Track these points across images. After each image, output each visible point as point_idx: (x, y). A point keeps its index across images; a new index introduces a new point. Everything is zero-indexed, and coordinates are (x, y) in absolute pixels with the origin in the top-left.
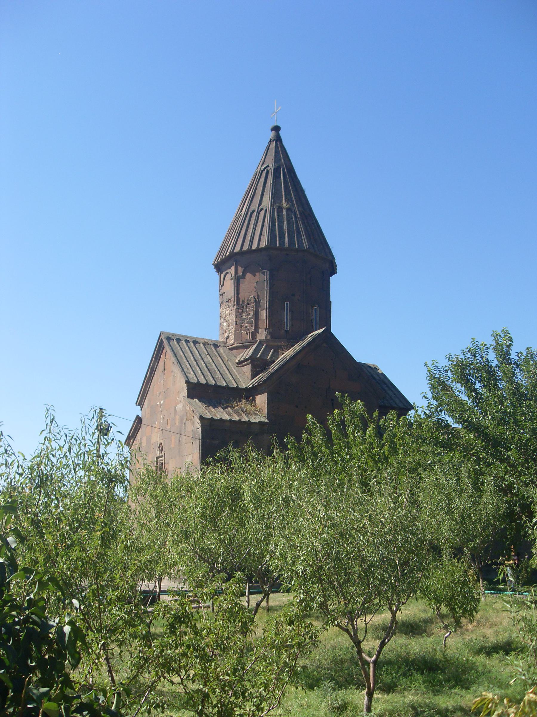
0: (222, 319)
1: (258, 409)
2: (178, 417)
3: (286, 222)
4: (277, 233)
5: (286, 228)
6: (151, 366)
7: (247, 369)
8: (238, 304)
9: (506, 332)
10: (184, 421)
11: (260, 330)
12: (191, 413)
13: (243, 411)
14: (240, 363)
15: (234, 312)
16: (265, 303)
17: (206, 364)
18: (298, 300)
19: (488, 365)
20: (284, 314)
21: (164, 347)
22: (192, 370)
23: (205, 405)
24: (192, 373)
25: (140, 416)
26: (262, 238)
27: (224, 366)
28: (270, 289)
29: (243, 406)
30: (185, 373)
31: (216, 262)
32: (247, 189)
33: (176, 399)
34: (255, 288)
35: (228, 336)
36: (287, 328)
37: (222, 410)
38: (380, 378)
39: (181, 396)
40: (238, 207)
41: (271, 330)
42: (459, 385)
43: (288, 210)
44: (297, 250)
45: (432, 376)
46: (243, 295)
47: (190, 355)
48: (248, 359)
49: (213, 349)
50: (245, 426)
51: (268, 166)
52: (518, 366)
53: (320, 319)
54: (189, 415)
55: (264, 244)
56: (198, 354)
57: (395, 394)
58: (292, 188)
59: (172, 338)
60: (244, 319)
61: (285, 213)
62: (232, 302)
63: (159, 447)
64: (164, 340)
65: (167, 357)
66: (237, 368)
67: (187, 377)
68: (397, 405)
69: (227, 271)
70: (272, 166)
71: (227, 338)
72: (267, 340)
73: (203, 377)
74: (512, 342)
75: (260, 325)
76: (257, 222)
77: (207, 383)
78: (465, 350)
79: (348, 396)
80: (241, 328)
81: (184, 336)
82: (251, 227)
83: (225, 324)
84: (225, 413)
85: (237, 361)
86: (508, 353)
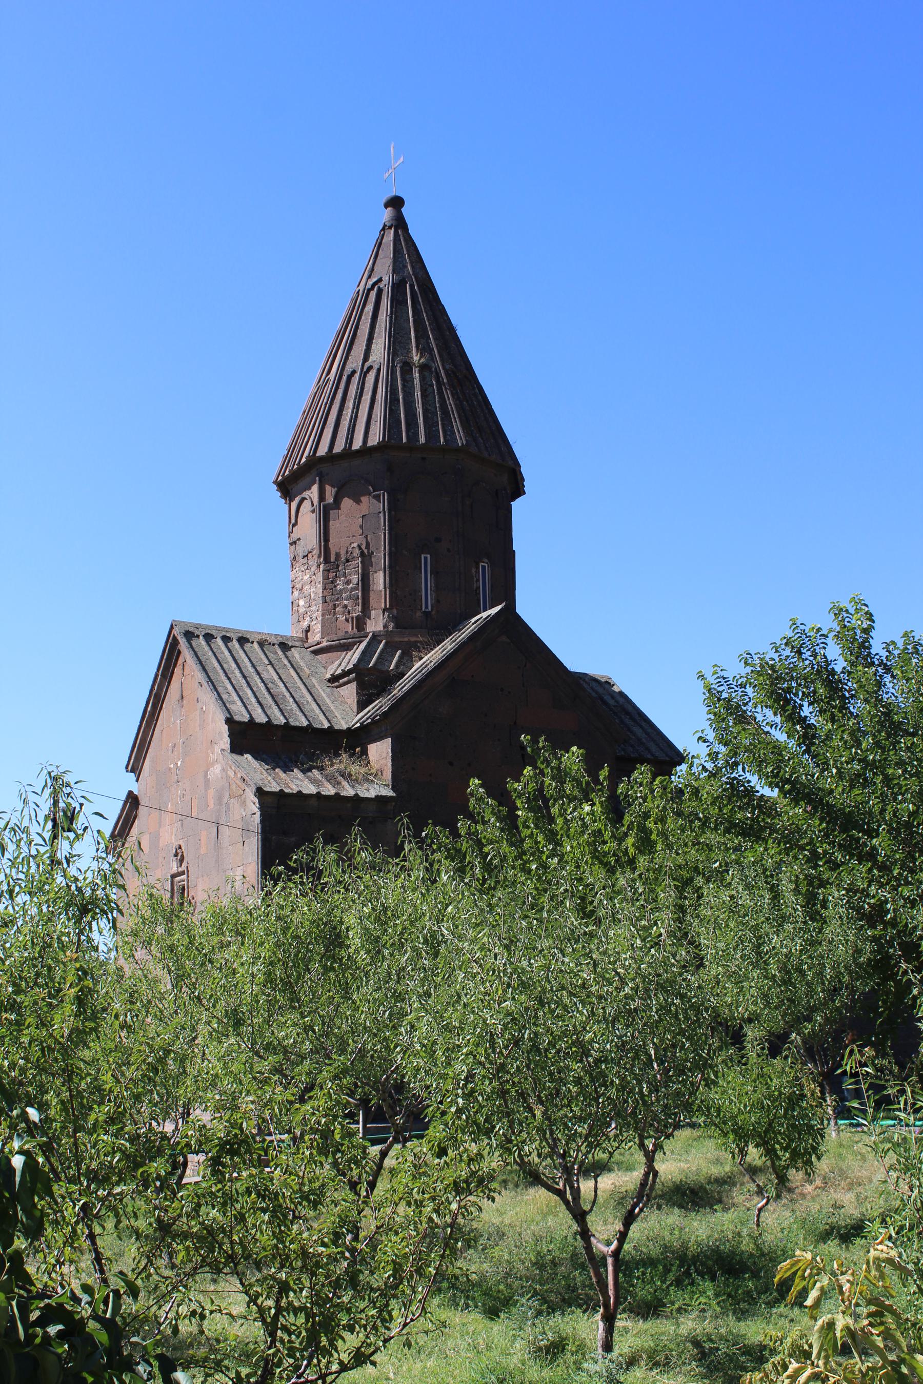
0: (296, 593)
1: (373, 771)
2: (212, 792)
3: (419, 393)
4: (402, 416)
5: (420, 405)
6: (154, 692)
7: (350, 692)
8: (327, 560)
9: (859, 603)
10: (225, 800)
11: (373, 613)
12: (239, 782)
13: (343, 776)
14: (334, 679)
15: (320, 577)
16: (381, 557)
17: (265, 685)
18: (449, 550)
19: (826, 669)
20: (421, 578)
21: (179, 652)
22: (239, 696)
23: (267, 767)
24: (239, 703)
25: (136, 793)
26: (372, 427)
27: (302, 687)
29: (342, 766)
31: (280, 478)
33: (208, 756)
34: (361, 527)
35: (309, 627)
36: (427, 607)
38: (617, 702)
40: (322, 365)
41: (395, 611)
42: (769, 713)
43: (423, 368)
44: (443, 450)
45: (713, 697)
47: (234, 666)
48: (350, 672)
49: (280, 652)
50: (349, 805)
51: (380, 280)
52: (888, 669)
54: (234, 787)
56: (249, 665)
57: (647, 734)
58: (430, 324)
59: (197, 632)
60: (341, 590)
61: (417, 375)
62: (315, 557)
63: (176, 855)
64: (179, 638)
66: (328, 690)
67: (228, 710)
68: (652, 755)
71: (307, 631)
72: (387, 631)
73: (260, 710)
74: (873, 622)
75: (372, 602)
77: (269, 722)
80: (335, 609)
82: (350, 404)
83: (302, 603)
84: (306, 781)
85: (328, 676)
86: (865, 645)
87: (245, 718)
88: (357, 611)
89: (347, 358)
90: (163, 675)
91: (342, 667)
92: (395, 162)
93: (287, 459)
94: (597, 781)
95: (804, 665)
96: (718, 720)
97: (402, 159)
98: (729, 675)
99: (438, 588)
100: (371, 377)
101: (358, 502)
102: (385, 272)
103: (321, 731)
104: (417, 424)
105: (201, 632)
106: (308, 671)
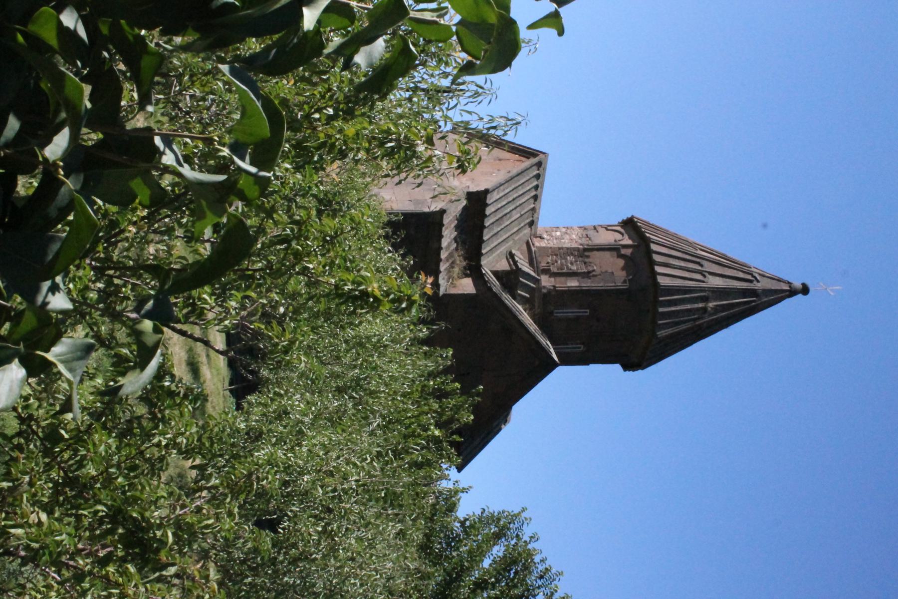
0: (564, 230)
7: (503, 265)
8: (585, 250)
11: (552, 279)
14: (512, 256)
15: (575, 245)
16: (587, 284)
17: (508, 213)
21: (528, 158)
22: (502, 197)
24: (498, 197)
26: (668, 278)
27: (507, 235)
28: (606, 291)
32: (730, 255)
34: (606, 272)
35: (543, 238)
36: (557, 313)
39: (468, 183)
41: (553, 293)
42: (501, 554)
43: (704, 310)
44: (654, 322)
47: (521, 193)
49: (528, 221)
51: (758, 281)
53: (568, 353)
55: (662, 281)
56: (521, 202)
59: (541, 169)
65: (518, 163)
67: (494, 190)
70: (758, 286)
71: (541, 238)
73: (493, 210)
77: (485, 216)
78: (548, 563)
79: (478, 401)
82: (682, 264)
83: (558, 234)
84: (449, 240)
85: (514, 252)
87: (489, 201)
88: (554, 269)
91: (519, 261)
94: (452, 434)
95: (531, 580)
96: (494, 519)
97: (832, 294)
101: (623, 269)
102: (763, 284)
103: (480, 248)
104: (669, 306)
105: (541, 171)
106: (517, 238)
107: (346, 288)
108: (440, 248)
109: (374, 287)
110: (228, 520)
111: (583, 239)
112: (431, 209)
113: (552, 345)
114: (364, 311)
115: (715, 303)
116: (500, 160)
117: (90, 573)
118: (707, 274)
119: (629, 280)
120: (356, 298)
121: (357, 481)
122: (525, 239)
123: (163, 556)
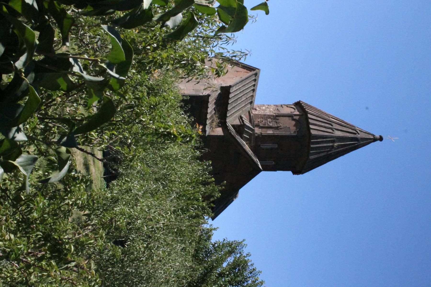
0: (267, 106)
1: (214, 129)
8: (277, 116)
11: (260, 130)
14: (241, 118)
15: (272, 114)
16: (277, 132)
17: (240, 97)
21: (251, 71)
24: (236, 89)
26: (316, 131)
29: (215, 120)
30: (236, 85)
32: (346, 121)
34: (286, 127)
37: (213, 107)
40: (335, 116)
41: (261, 136)
42: (232, 261)
43: (333, 147)
46: (282, 119)
47: (246, 88)
49: (249, 101)
51: (359, 134)
55: (313, 132)
56: (246, 92)
62: (277, 113)
67: (234, 86)
69: (296, 109)
70: (359, 136)
71: (256, 110)
73: (233, 95)
76: (326, 128)
81: (257, 85)
82: (323, 124)
83: (264, 108)
84: (211, 109)
85: (242, 116)
87: (231, 91)
88: (261, 125)
89: (336, 123)
90: (244, 66)
91: (245, 120)
92: (393, 139)
93: (307, 105)
94: (210, 203)
97: (394, 141)
98: (244, 249)
99: (267, 149)
100: (330, 131)
101: (294, 126)
102: (361, 135)
103: (226, 114)
104: (316, 144)
105: (256, 78)
106: (244, 109)
107: (160, 130)
108: (207, 113)
109: (174, 130)
110: (101, 241)
111: (276, 111)
112: (203, 94)
113: (259, 161)
114: (169, 142)
115: (338, 144)
116: (237, 72)
117: (34, 265)
118: (334, 130)
119: (297, 131)
120: (165, 136)
121: (163, 224)
122: (248, 110)
123: (69, 257)
